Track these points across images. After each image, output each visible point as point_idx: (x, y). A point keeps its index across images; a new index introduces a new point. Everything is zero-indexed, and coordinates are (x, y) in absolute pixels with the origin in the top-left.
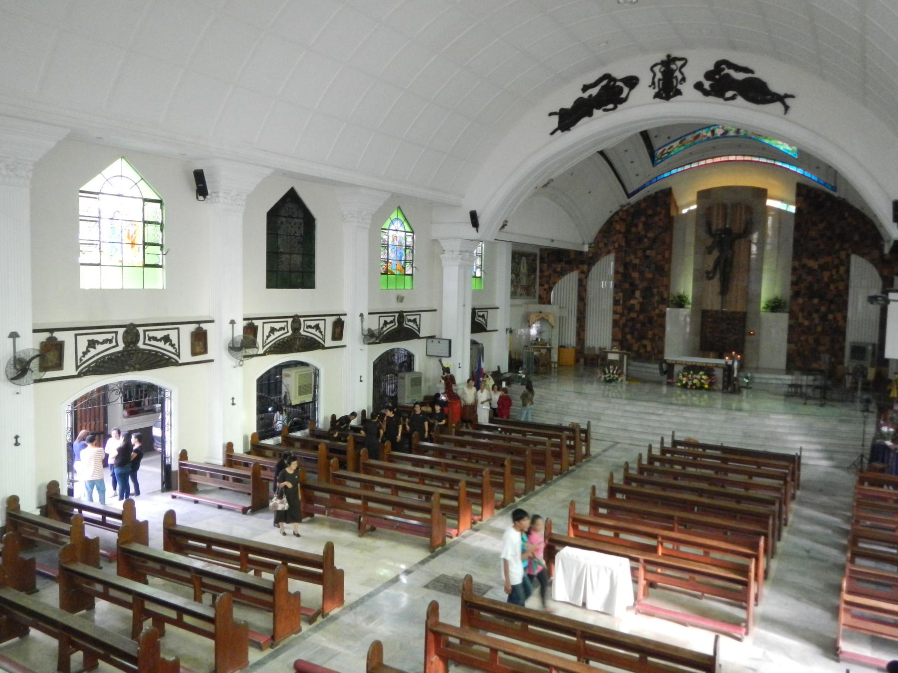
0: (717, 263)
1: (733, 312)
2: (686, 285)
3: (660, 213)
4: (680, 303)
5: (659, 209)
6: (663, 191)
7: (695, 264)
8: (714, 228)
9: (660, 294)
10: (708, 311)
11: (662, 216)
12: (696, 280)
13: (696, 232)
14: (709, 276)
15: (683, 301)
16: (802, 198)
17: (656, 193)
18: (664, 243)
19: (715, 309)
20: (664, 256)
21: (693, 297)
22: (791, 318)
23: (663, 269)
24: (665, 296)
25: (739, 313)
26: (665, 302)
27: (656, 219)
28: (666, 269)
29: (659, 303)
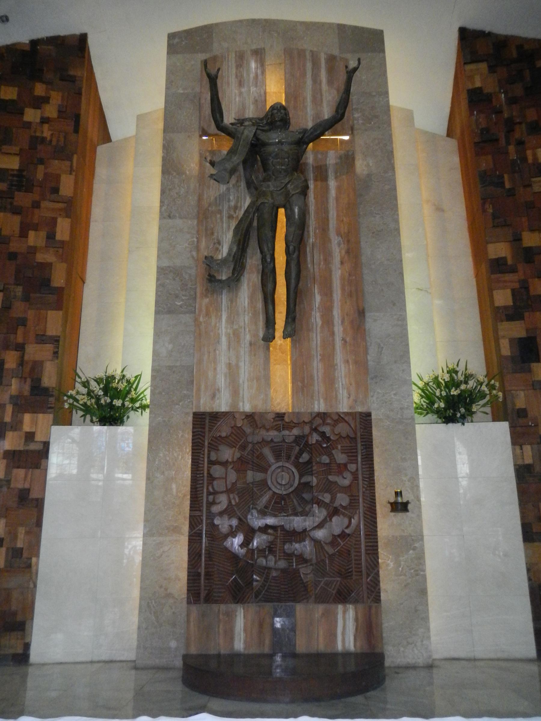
0: (253, 231)
1: (323, 416)
2: (124, 328)
3: (46, 100)
4: (110, 406)
5: (40, 89)
6: (57, 41)
7: (161, 253)
8: (229, 119)
9: (32, 373)
10: (215, 416)
11: (51, 110)
12: (164, 307)
13: (168, 147)
14: (218, 277)
15: (117, 394)
16: (483, 66)
17: (34, 43)
18: (56, 190)
19: (247, 407)
20: (51, 236)
21: (156, 373)
22: (518, 438)
23: (46, 283)
24: (49, 379)
25: (340, 418)
26: (47, 400)
27: (31, 115)
28: (58, 279)
29: (22, 405)
